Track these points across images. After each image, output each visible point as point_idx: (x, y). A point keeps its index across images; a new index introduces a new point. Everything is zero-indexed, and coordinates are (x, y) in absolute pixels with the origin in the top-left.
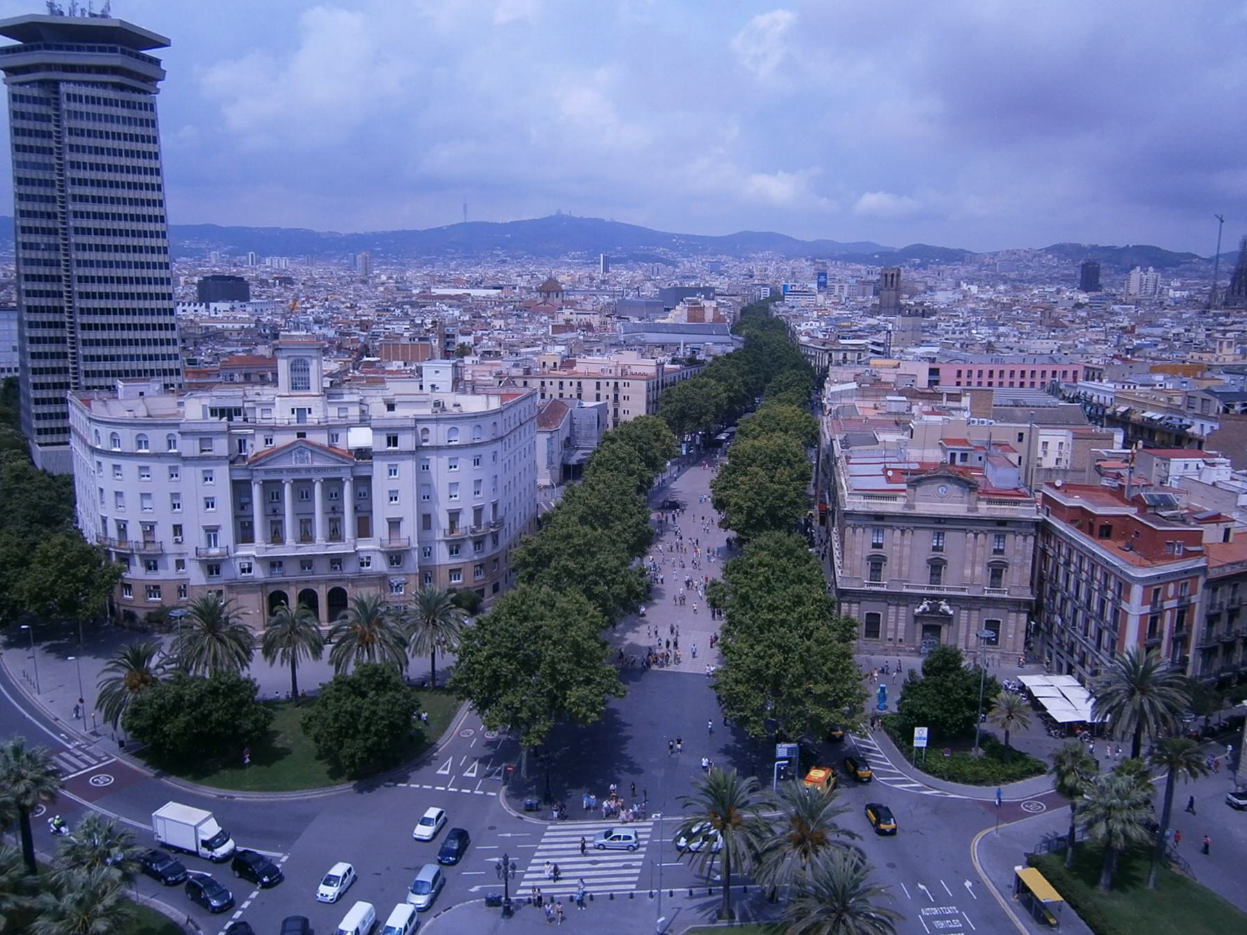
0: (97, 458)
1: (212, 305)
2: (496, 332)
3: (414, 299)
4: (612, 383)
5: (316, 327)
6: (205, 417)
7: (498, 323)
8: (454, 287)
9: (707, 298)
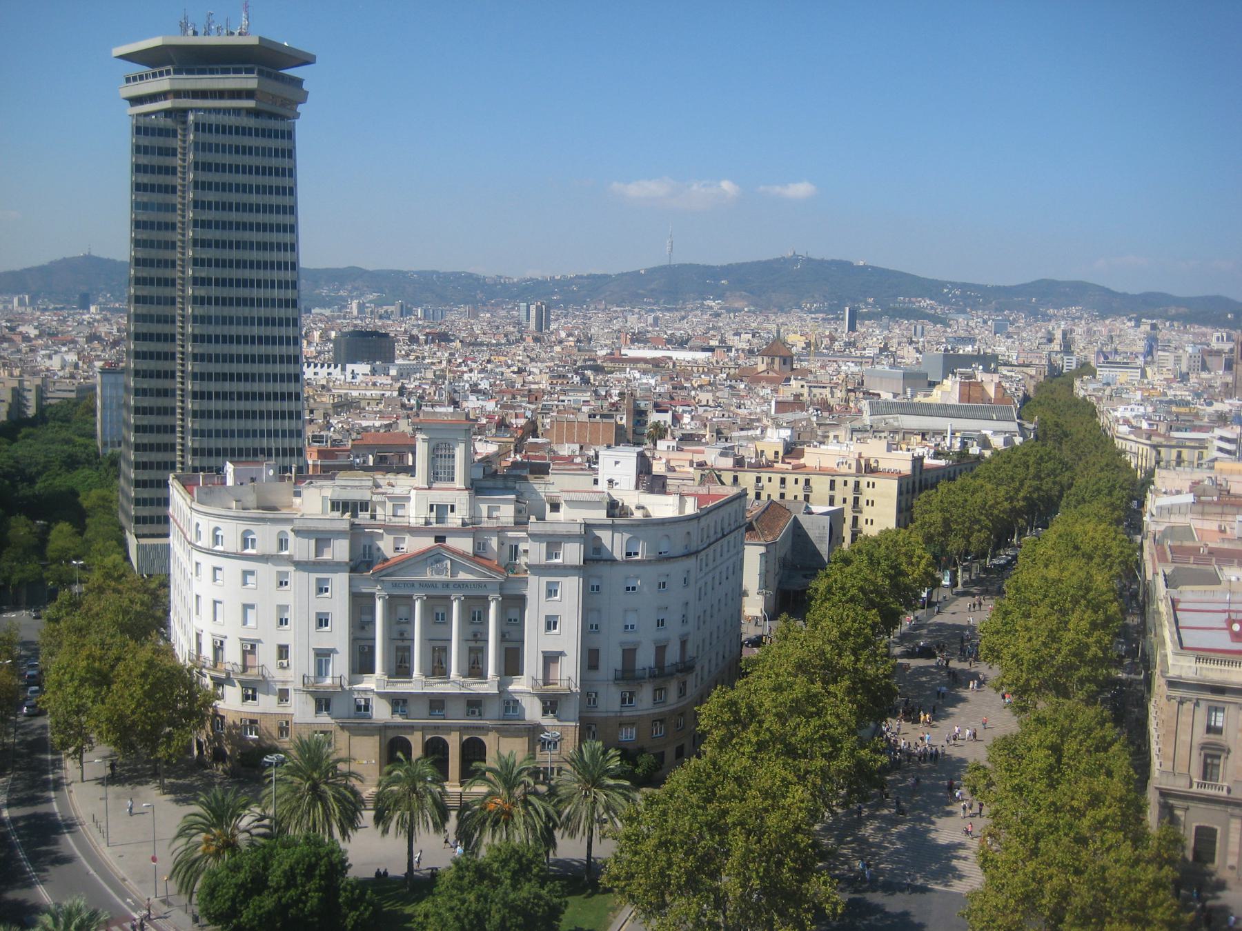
0: (197, 556)
1: (349, 367)
2: (701, 410)
3: (599, 362)
4: (851, 481)
5: (473, 398)
6: (324, 512)
7: (704, 397)
8: (649, 348)
9: (987, 370)
